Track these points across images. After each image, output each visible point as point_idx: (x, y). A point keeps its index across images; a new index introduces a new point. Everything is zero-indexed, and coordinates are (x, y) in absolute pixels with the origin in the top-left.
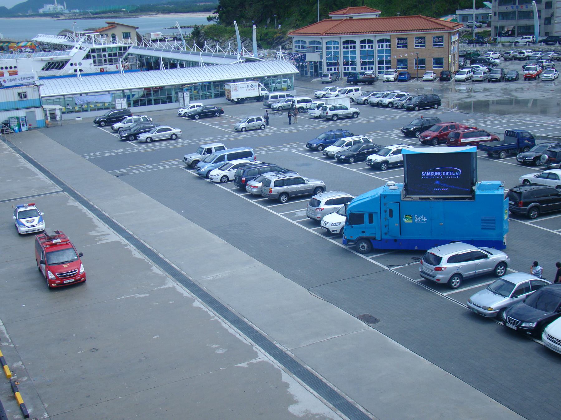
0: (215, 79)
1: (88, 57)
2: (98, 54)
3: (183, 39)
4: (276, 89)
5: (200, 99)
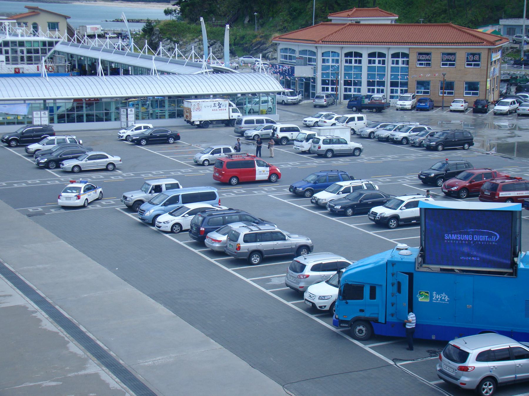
0: (171, 93)
2: (12, 49)
3: (130, 36)
4: (252, 111)
5: (149, 118)
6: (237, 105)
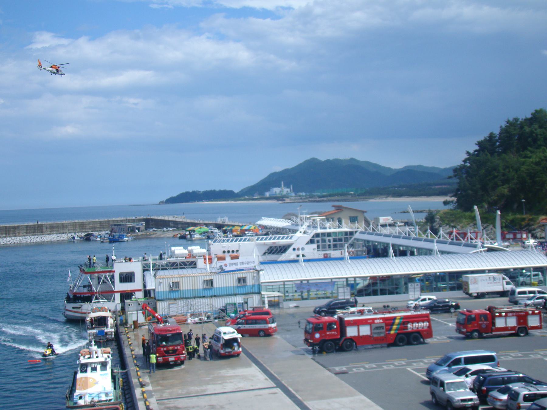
1: (311, 242)
2: (322, 239)
3: (415, 224)
4: (524, 283)
6: (510, 278)
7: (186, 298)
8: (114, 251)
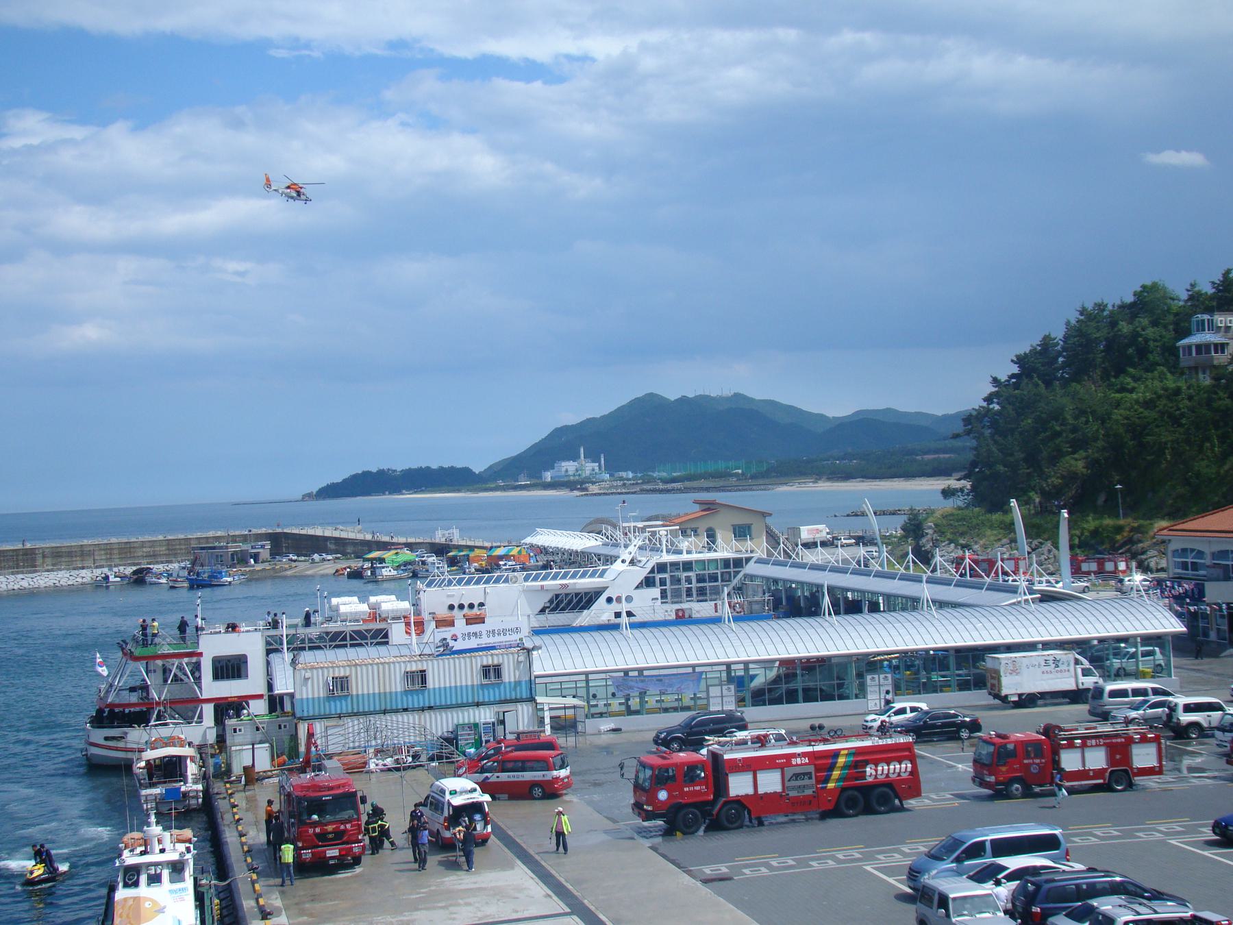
0: (960, 643)
1: (648, 582)
2: (671, 576)
3: (879, 541)
4: (1122, 672)
7: (365, 714)
8: (199, 608)
